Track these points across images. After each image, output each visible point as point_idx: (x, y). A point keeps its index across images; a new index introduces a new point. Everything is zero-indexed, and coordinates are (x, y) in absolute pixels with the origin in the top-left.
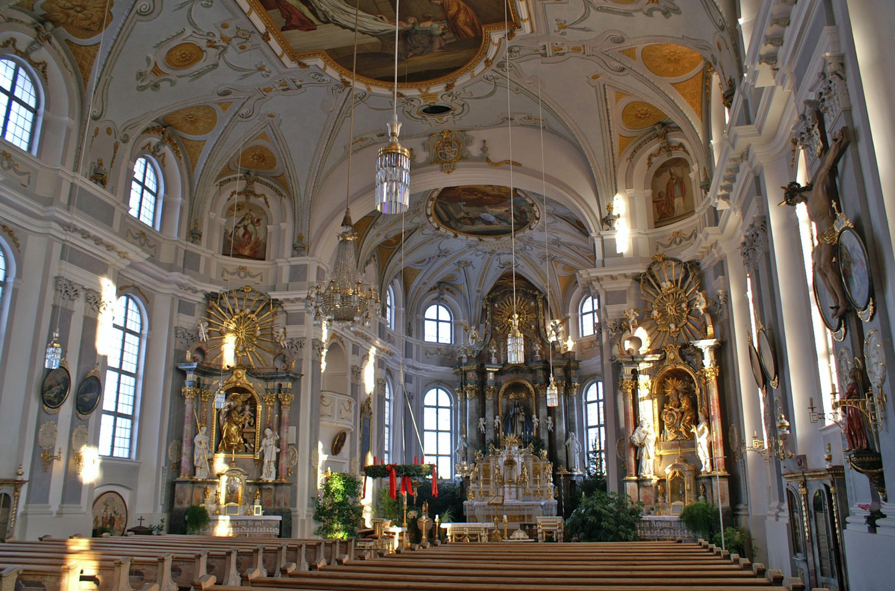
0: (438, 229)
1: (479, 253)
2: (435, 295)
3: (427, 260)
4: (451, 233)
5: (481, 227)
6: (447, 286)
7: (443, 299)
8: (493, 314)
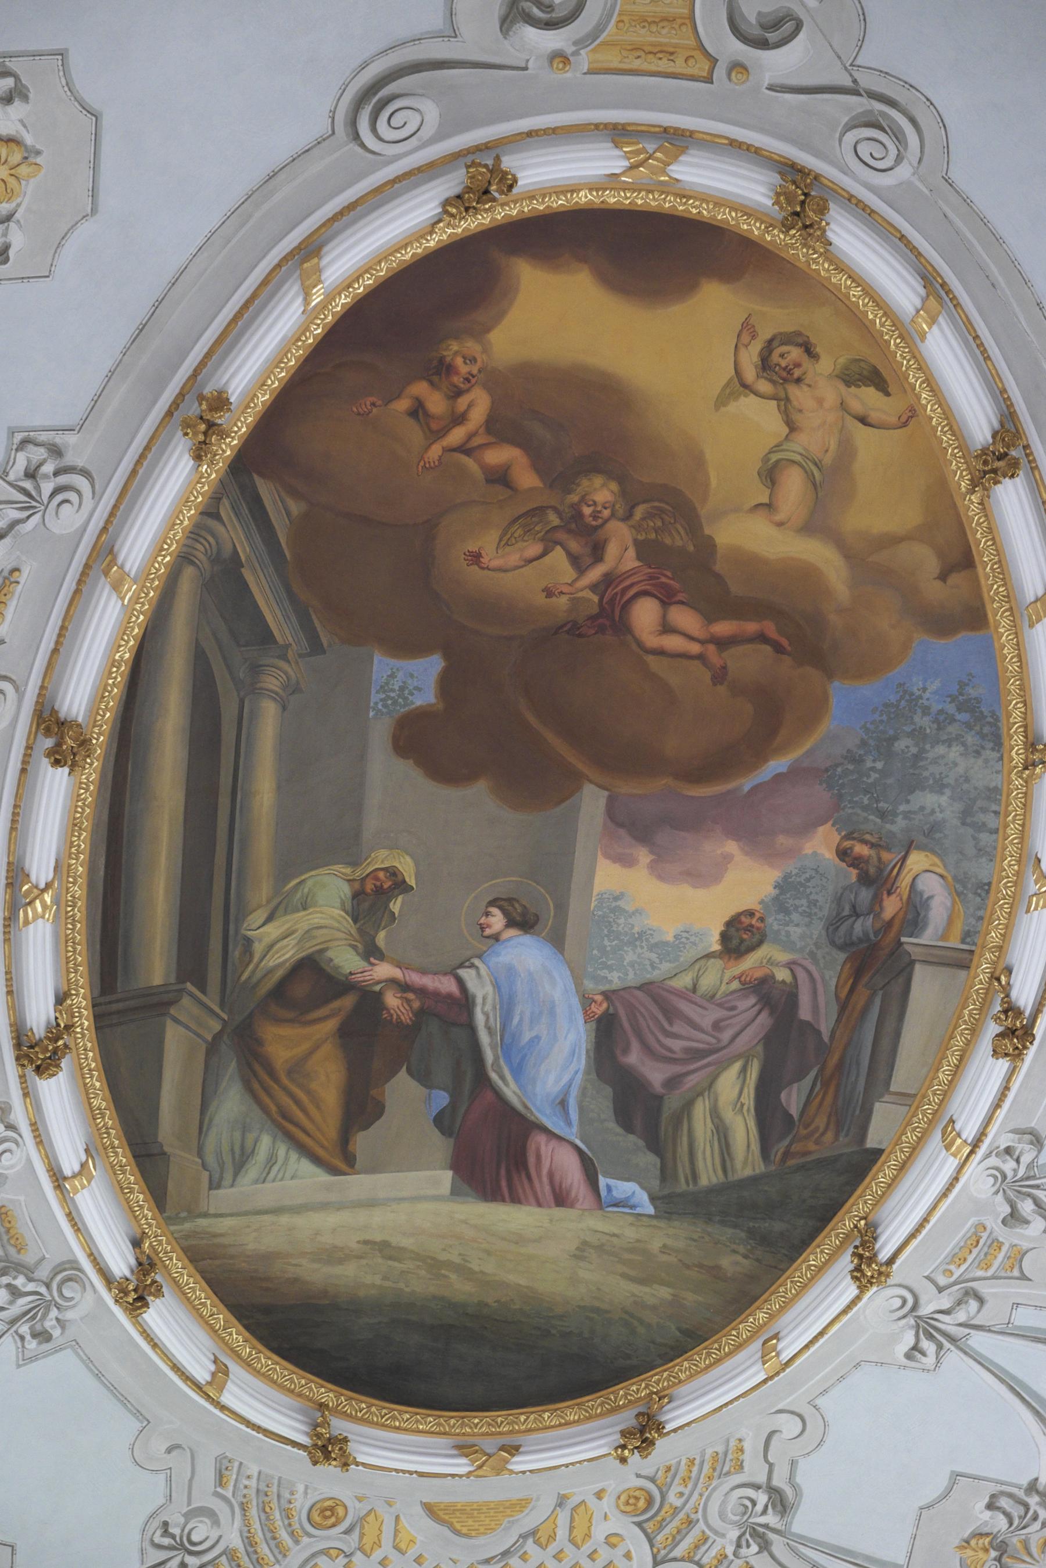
4: (104, 1224)
5: (391, 1216)
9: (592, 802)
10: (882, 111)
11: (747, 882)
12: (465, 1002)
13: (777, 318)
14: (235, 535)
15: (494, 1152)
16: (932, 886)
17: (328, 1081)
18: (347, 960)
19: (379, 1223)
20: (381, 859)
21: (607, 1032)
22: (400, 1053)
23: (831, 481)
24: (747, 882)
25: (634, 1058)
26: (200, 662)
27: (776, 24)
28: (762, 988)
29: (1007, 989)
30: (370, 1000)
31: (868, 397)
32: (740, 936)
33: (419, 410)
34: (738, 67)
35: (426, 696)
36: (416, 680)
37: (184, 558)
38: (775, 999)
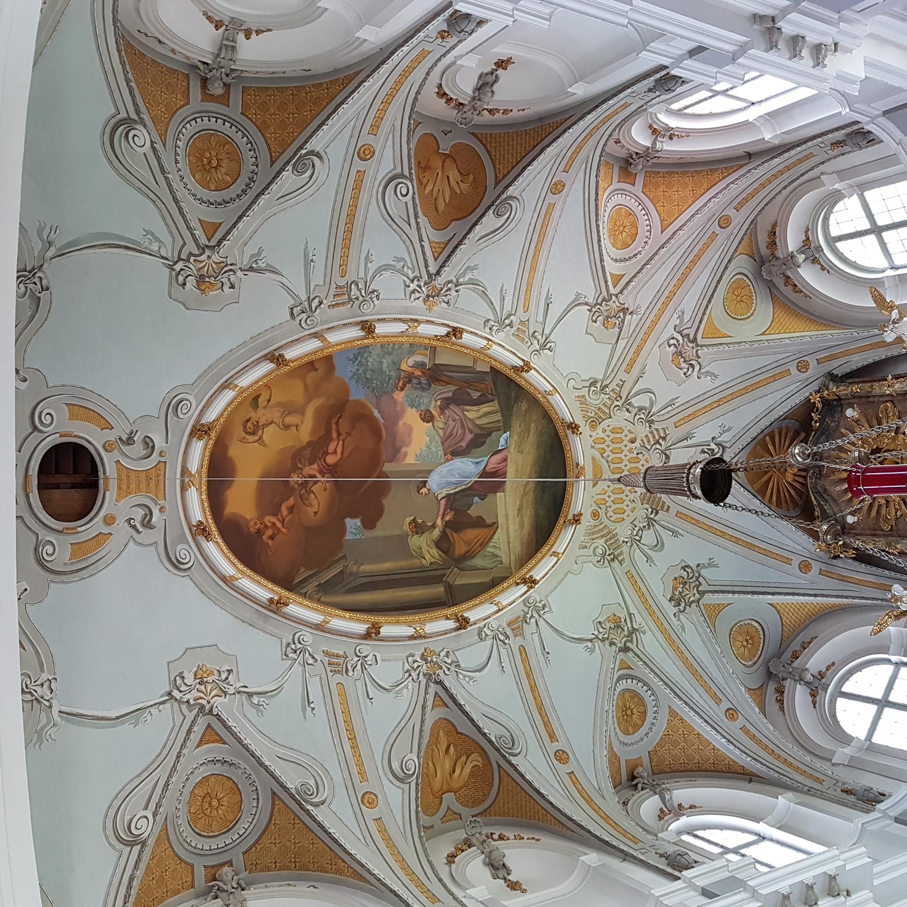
0: (463, 623)
1: (648, 537)
2: (800, 695)
3: (624, 684)
6: (788, 654)
7: (822, 675)
8: (874, 532)
9: (388, 467)
10: (173, 406)
11: (411, 417)
12: (448, 496)
13: (239, 432)
14: (311, 587)
15: (490, 483)
16: (411, 362)
17: (471, 534)
18: (436, 533)
19: (512, 512)
20: (406, 527)
21: (456, 453)
22: (463, 513)
23: (288, 409)
24: (411, 417)
25: (464, 444)
26: (348, 592)
27: (147, 444)
28: (442, 409)
29: (442, 336)
30: (447, 525)
31: (262, 401)
32: (427, 417)
33: (272, 537)
34: (161, 454)
35: (358, 522)
36: (353, 524)
37: (319, 601)
38: (446, 404)
